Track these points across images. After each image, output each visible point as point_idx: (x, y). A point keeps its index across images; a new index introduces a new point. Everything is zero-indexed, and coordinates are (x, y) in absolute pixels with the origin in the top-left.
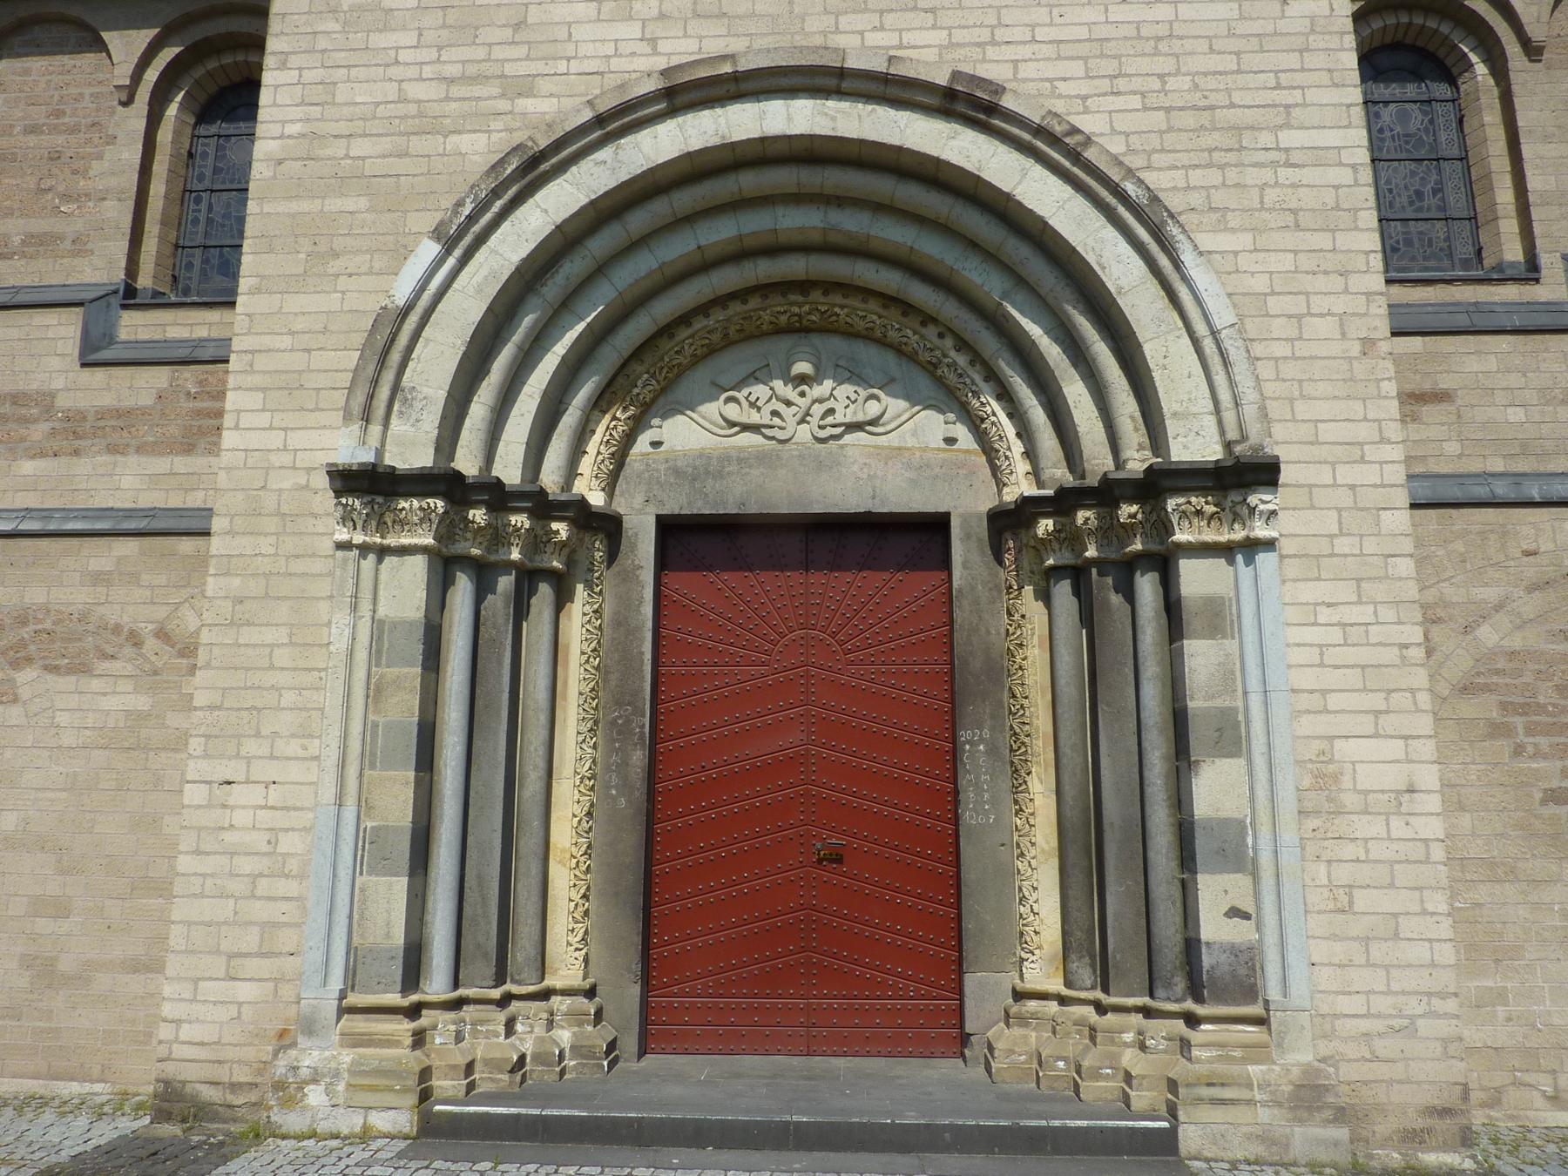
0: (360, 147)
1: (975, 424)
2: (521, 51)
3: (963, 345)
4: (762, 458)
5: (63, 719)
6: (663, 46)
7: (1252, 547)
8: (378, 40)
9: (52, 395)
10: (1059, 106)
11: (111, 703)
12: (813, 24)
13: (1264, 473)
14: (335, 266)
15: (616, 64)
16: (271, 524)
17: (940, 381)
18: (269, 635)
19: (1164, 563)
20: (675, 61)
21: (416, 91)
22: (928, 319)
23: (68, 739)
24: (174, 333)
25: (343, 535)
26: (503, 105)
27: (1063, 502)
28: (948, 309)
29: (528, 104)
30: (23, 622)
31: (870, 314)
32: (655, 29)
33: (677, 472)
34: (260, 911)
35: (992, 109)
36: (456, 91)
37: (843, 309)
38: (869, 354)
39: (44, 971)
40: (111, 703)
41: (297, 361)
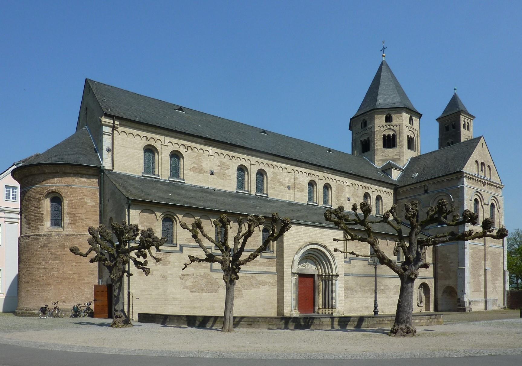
0: (290, 246)
1: (317, 267)
2: (299, 239)
3: (318, 262)
4: (305, 269)
5: (264, 289)
6: (308, 240)
7: (337, 280)
8: (291, 236)
9: (258, 261)
10: (329, 247)
11: (267, 288)
12: (317, 239)
13: (338, 276)
14: (290, 256)
15: (305, 241)
16: (287, 276)
17: (315, 264)
18: (288, 284)
19: (332, 280)
20: (309, 241)
21: (294, 241)
22: (316, 259)
23: (264, 291)
24: (266, 255)
25: (292, 277)
26: (299, 243)
27: (325, 275)
28: (318, 260)
29: (300, 243)
30: (260, 281)
31: (312, 258)
32: (308, 238)
33: (299, 270)
34: (289, 304)
35: (326, 248)
36: (296, 242)
37: (311, 258)
38: (311, 261)
39: (264, 310)
40: (267, 288)
41: (288, 263)
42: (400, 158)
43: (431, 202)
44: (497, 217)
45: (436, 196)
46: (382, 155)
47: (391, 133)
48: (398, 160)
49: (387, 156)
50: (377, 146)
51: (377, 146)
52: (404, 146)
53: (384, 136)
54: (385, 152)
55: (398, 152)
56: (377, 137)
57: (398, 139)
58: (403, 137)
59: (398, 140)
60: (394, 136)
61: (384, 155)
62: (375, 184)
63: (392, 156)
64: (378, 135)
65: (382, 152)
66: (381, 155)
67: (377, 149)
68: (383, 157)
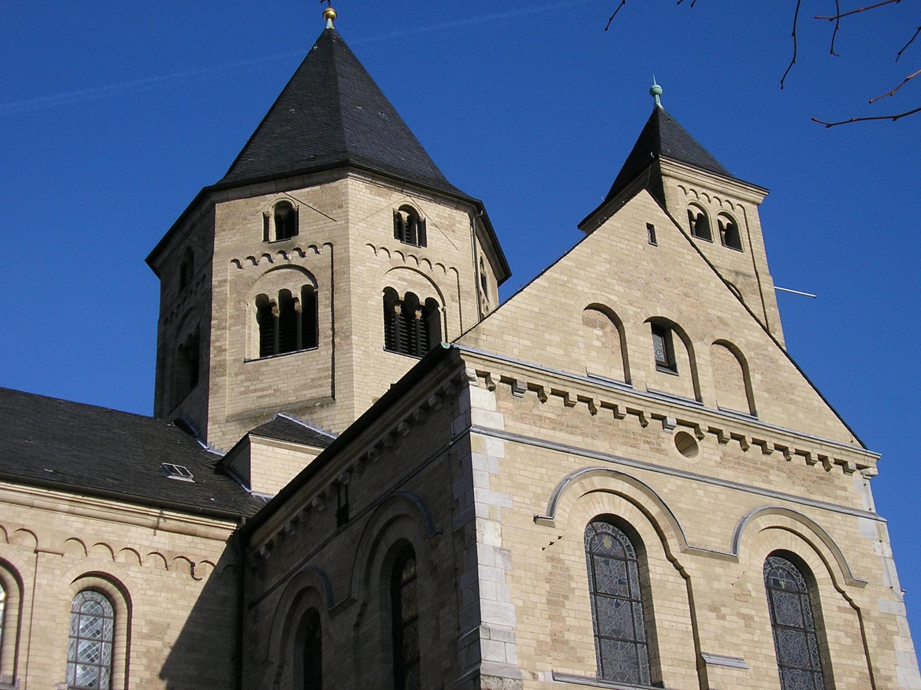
42: (333, 396)
43: (359, 575)
44: (848, 641)
45: (375, 533)
46: (245, 393)
47: (296, 286)
48: (322, 406)
49: (269, 396)
50: (222, 350)
51: (222, 350)
52: (353, 337)
53: (264, 305)
54: (263, 373)
55: (327, 370)
56: (221, 308)
57: (326, 306)
58: (349, 292)
59: (323, 311)
60: (310, 296)
61: (256, 390)
62: (64, 506)
63: (294, 390)
64: (224, 301)
65: (243, 377)
66: (241, 393)
67: (222, 365)
68: (251, 403)
